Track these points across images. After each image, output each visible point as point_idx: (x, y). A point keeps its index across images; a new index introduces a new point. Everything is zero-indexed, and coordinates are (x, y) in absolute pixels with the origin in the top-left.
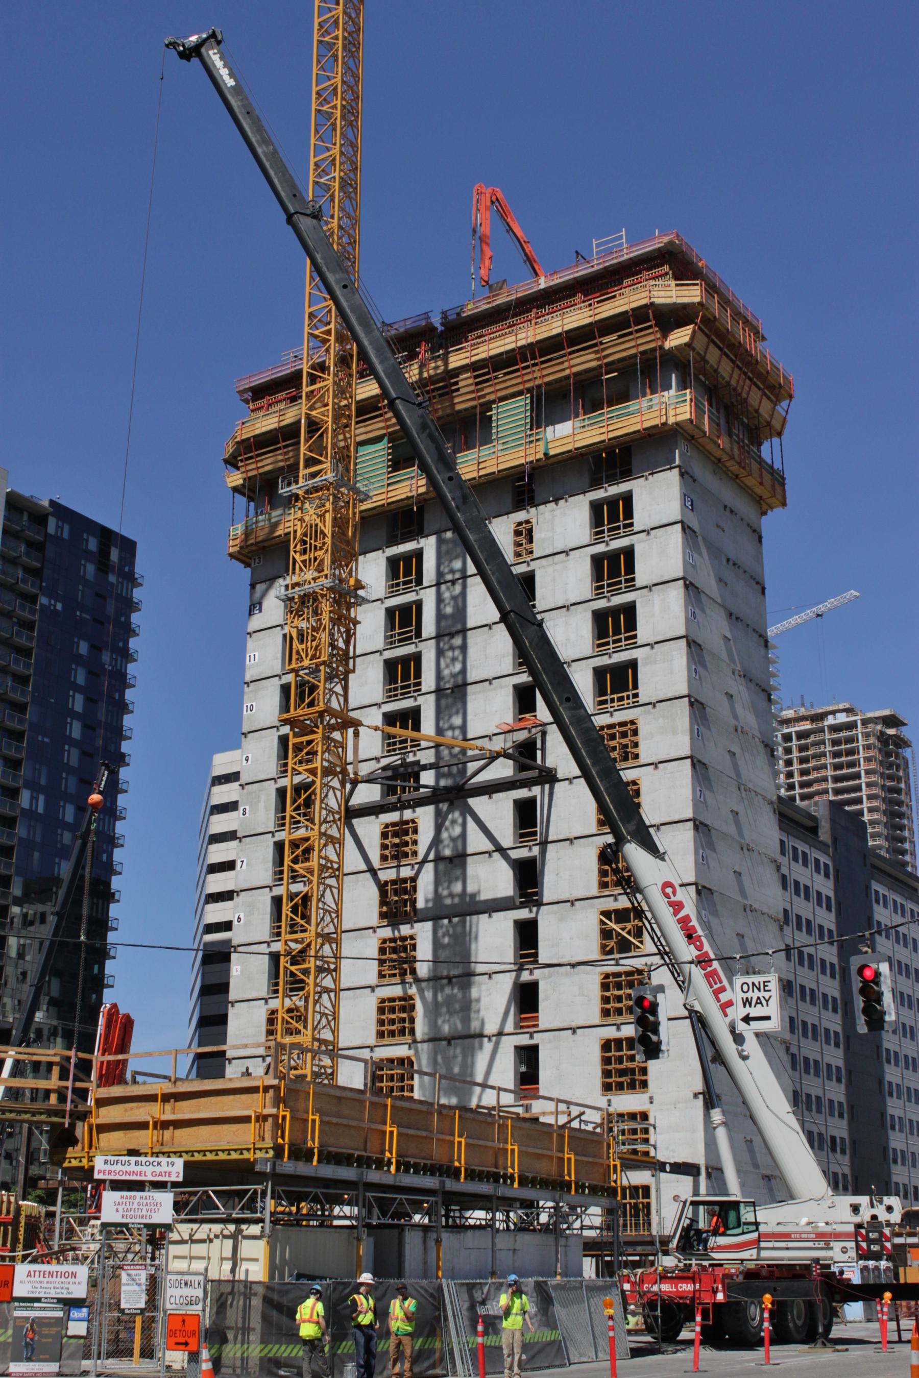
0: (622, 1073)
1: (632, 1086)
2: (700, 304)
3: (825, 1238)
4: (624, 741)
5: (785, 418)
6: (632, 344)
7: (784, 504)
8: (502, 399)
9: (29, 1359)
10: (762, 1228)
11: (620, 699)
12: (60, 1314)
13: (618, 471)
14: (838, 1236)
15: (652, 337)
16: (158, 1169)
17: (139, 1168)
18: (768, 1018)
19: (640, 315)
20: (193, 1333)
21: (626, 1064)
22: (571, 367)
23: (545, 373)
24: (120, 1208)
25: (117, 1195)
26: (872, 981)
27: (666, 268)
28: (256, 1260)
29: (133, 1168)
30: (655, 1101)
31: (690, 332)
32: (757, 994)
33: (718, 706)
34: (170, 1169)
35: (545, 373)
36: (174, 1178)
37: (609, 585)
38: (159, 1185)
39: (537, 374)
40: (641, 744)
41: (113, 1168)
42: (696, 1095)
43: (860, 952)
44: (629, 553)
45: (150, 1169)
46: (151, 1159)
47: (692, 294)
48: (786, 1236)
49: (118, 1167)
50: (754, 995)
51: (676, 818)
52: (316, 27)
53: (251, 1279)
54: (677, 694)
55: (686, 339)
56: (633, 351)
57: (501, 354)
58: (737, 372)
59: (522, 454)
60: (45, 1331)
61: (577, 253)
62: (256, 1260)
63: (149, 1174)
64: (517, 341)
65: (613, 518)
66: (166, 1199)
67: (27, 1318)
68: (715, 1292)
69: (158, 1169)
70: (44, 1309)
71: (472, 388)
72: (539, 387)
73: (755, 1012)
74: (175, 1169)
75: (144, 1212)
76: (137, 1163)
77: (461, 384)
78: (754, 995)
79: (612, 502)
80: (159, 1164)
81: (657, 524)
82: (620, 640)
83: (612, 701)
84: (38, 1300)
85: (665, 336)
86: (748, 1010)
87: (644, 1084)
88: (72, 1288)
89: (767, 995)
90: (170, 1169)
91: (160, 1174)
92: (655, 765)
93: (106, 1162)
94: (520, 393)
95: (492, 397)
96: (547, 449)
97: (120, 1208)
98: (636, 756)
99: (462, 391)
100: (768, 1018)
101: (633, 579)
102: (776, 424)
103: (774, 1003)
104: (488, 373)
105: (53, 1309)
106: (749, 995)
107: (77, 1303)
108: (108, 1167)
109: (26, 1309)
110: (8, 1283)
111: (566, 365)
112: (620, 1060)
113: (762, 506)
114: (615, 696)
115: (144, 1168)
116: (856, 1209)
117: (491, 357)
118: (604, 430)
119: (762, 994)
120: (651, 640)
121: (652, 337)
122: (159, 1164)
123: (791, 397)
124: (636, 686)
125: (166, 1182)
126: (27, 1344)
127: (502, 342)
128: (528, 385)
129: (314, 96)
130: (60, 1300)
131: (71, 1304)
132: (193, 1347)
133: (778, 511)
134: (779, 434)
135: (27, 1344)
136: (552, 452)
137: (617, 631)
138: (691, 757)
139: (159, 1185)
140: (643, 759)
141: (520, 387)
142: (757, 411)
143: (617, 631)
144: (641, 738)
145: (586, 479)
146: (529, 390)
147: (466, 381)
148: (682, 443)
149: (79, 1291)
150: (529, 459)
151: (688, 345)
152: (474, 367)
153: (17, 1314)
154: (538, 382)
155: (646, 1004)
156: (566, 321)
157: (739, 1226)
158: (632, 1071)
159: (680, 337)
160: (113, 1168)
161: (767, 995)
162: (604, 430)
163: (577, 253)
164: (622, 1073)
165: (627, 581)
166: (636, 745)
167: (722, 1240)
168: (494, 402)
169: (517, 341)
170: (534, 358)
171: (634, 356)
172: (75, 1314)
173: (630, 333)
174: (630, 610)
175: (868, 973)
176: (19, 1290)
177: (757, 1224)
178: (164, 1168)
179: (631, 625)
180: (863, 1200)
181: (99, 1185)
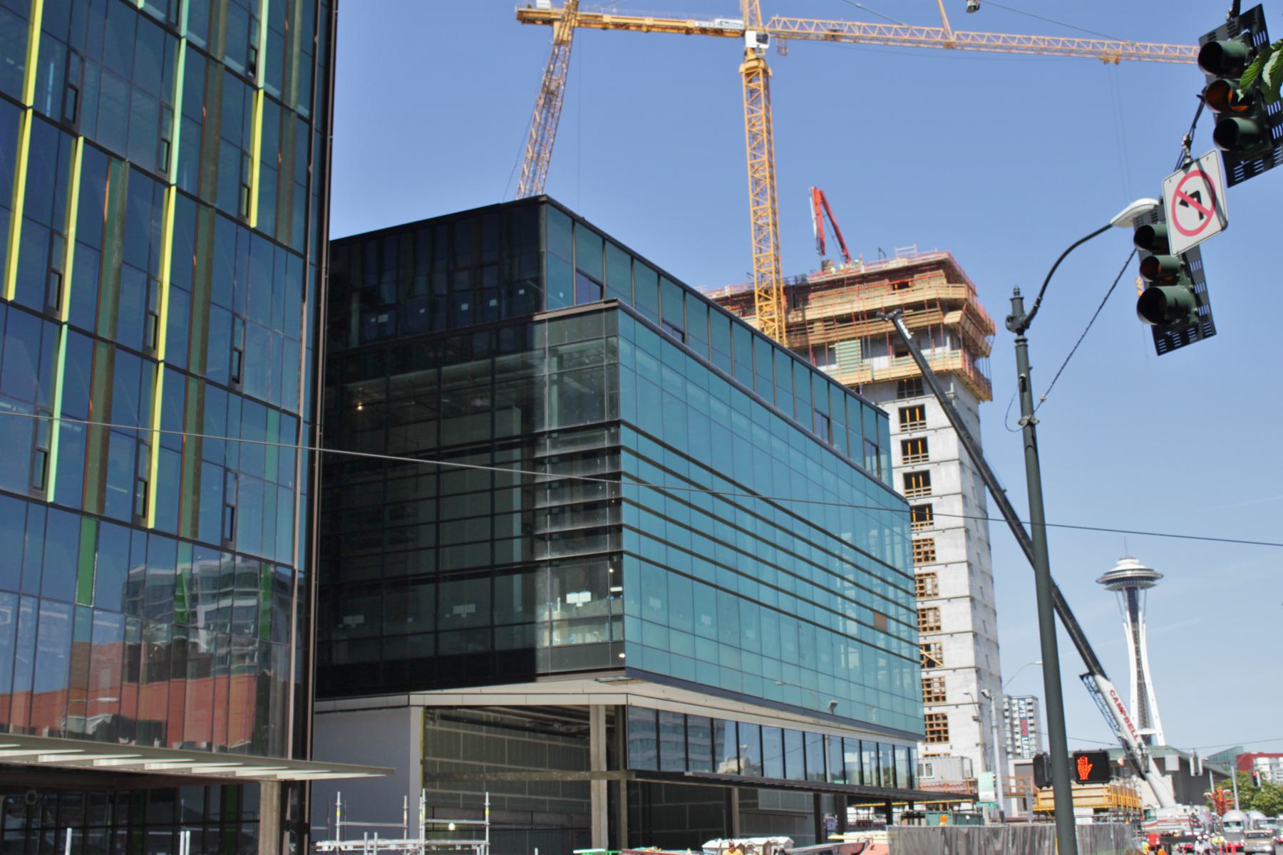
0: (932, 732)
1: (939, 739)
2: (966, 299)
3: (1179, 821)
4: (926, 549)
5: (991, 348)
6: (925, 319)
7: (991, 400)
8: (842, 340)
10: (1158, 819)
11: (922, 525)
13: (914, 390)
14: (1184, 820)
15: (937, 317)
19: (931, 304)
21: (935, 728)
22: (886, 328)
23: (870, 329)
27: (941, 272)
30: (954, 747)
31: (960, 315)
33: (973, 532)
35: (870, 329)
37: (912, 458)
39: (864, 329)
40: (937, 552)
42: (977, 745)
44: (924, 441)
47: (958, 293)
48: (1165, 821)
51: (960, 595)
52: (746, 121)
54: (957, 526)
55: (957, 319)
56: (926, 324)
57: (842, 315)
58: (972, 326)
59: (857, 376)
61: (880, 249)
64: (852, 308)
65: (913, 418)
68: (1155, 841)
71: (823, 332)
72: (866, 337)
77: (815, 329)
79: (912, 410)
81: (942, 426)
82: (920, 491)
83: (917, 526)
85: (944, 314)
87: (946, 739)
92: (946, 565)
94: (854, 339)
95: (835, 339)
96: (873, 376)
98: (934, 559)
99: (815, 333)
101: (927, 456)
102: (987, 353)
104: (834, 324)
111: (883, 326)
112: (931, 726)
113: (979, 399)
114: (919, 523)
116: (1185, 810)
117: (836, 316)
118: (908, 369)
120: (941, 493)
121: (937, 317)
123: (994, 334)
124: (931, 518)
127: (843, 307)
128: (859, 335)
129: (749, 167)
133: (987, 403)
134: (987, 356)
136: (876, 378)
137: (918, 485)
138: (967, 562)
140: (938, 560)
141: (853, 336)
142: (981, 348)
143: (918, 485)
144: (937, 547)
145: (895, 393)
146: (860, 338)
147: (818, 327)
148: (954, 378)
150: (862, 380)
151: (959, 323)
152: (825, 320)
154: (865, 334)
156: (884, 300)
157: (1150, 817)
158: (939, 732)
159: (953, 317)
162: (908, 369)
163: (880, 249)
164: (932, 732)
165: (923, 457)
166: (933, 552)
167: (1146, 823)
168: (836, 342)
169: (852, 308)
170: (863, 319)
171: (927, 326)
173: (925, 313)
174: (926, 475)
177: (1155, 817)
179: (927, 482)
180: (1188, 807)
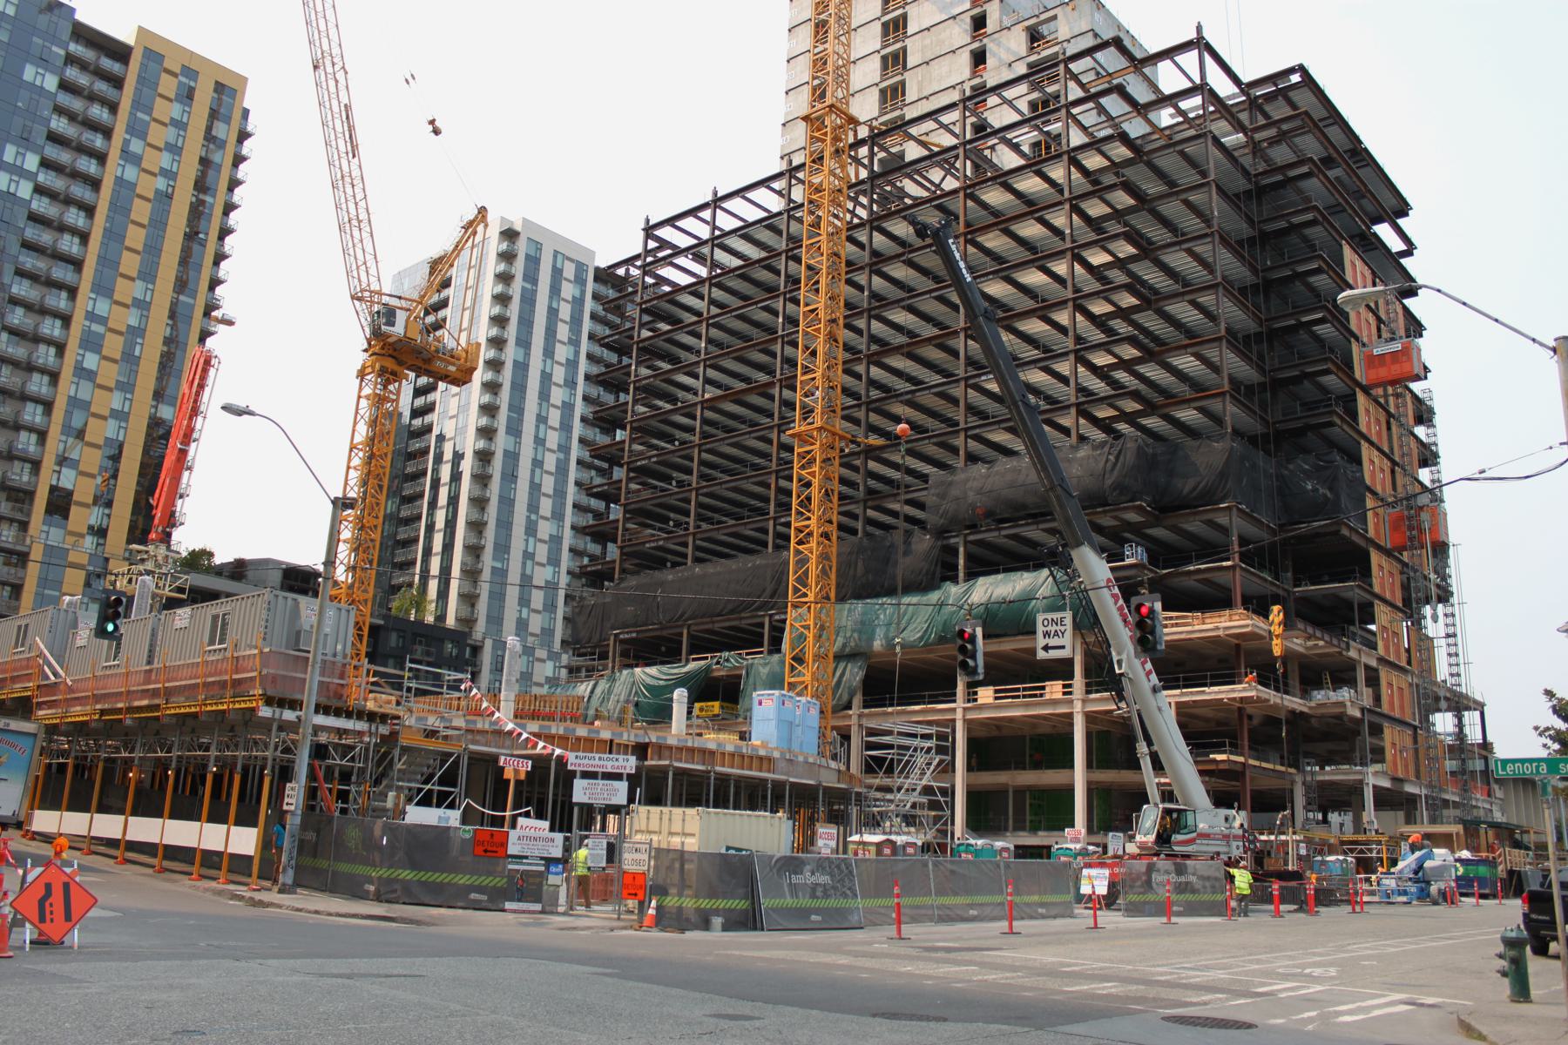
9: (519, 900)
12: (543, 868)
16: (616, 764)
17: (602, 763)
18: (1063, 647)
20: (641, 887)
25: (585, 782)
26: (1148, 617)
28: (694, 835)
29: (597, 762)
32: (1055, 627)
36: (628, 771)
38: (617, 777)
43: (1138, 593)
45: (610, 763)
49: (586, 762)
50: (1052, 628)
53: (686, 849)
60: (531, 880)
62: (694, 835)
66: (622, 787)
67: (518, 871)
69: (616, 764)
70: (530, 864)
73: (1053, 642)
78: (1052, 628)
84: (526, 857)
86: (1047, 641)
88: (551, 850)
89: (1063, 628)
100: (1063, 647)
103: (1069, 634)
105: (537, 865)
106: (1048, 629)
107: (555, 861)
108: (578, 761)
109: (517, 863)
110: (504, 844)
115: (605, 763)
119: (1058, 628)
125: (621, 774)
126: (518, 890)
130: (542, 858)
131: (549, 861)
132: (640, 896)
135: (518, 890)
139: (617, 777)
149: (557, 852)
153: (510, 867)
155: (966, 635)
161: (1063, 628)
172: (553, 869)
175: (1144, 610)
176: (512, 850)
178: (621, 763)
181: (573, 774)
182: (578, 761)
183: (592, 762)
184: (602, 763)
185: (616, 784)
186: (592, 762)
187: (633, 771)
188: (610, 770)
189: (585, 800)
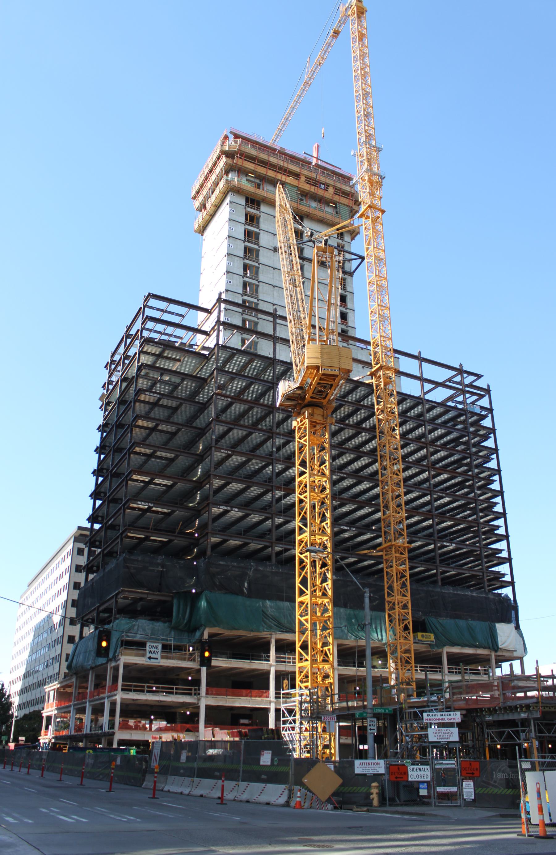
16: (450, 717)
17: (442, 717)
24: (436, 735)
29: (439, 717)
34: (455, 717)
38: (451, 725)
41: (431, 718)
45: (446, 717)
46: (447, 713)
49: (433, 717)
63: (446, 719)
66: (455, 730)
69: (450, 717)
74: (457, 717)
75: (446, 737)
76: (441, 715)
80: (450, 715)
90: (455, 717)
91: (451, 719)
93: (428, 715)
97: (436, 735)
108: (429, 717)
115: (444, 717)
122: (450, 715)
139: (451, 725)
160: (431, 718)
178: (452, 716)
182: (429, 717)
183: (436, 717)
184: (442, 717)
185: (451, 729)
186: (436, 717)
187: (460, 721)
188: (447, 721)
189: (435, 739)
